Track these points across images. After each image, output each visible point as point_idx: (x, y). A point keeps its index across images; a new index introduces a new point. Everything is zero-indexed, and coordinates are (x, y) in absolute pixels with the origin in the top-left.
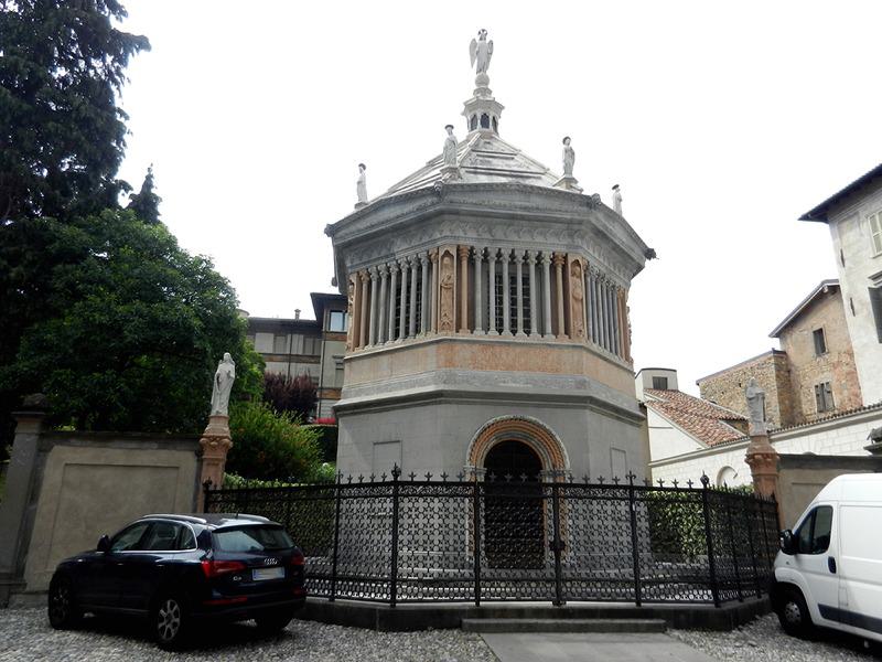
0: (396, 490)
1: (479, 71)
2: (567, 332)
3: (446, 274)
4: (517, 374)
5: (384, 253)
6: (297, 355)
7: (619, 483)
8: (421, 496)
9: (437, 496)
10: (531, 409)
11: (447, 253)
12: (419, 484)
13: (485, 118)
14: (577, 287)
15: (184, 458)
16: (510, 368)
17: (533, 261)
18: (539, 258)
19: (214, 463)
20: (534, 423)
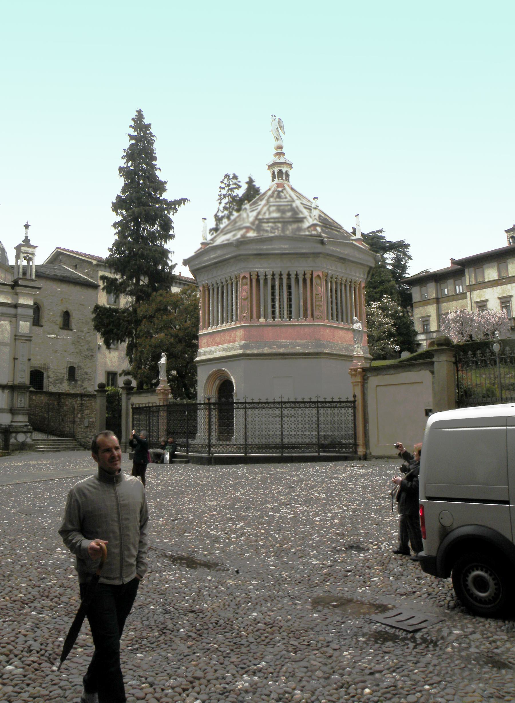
11: (244, 277)
13: (280, 172)
17: (293, 277)
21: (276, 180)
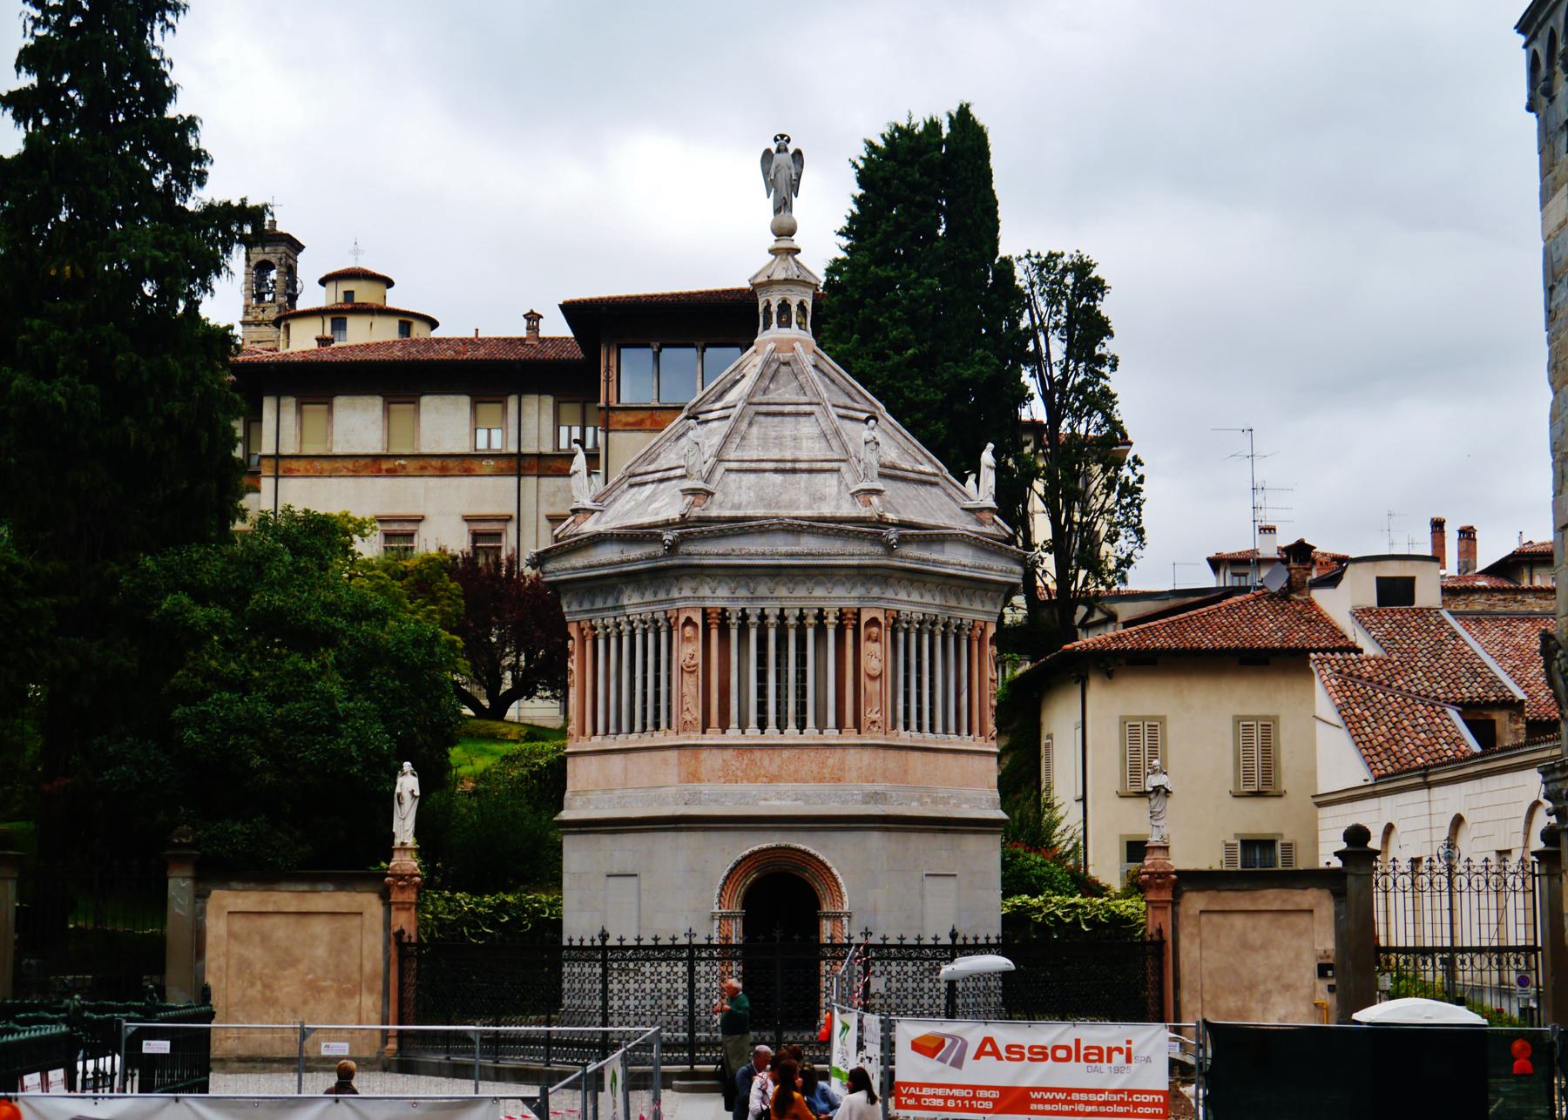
0: (604, 955)
1: (777, 211)
2: (857, 724)
3: (688, 651)
4: (783, 787)
5: (610, 603)
6: (540, 456)
8: (631, 960)
11: (689, 621)
12: (628, 948)
14: (874, 656)
15: (369, 903)
16: (773, 779)
18: (821, 616)
19: (404, 906)
20: (804, 852)
21: (774, 325)
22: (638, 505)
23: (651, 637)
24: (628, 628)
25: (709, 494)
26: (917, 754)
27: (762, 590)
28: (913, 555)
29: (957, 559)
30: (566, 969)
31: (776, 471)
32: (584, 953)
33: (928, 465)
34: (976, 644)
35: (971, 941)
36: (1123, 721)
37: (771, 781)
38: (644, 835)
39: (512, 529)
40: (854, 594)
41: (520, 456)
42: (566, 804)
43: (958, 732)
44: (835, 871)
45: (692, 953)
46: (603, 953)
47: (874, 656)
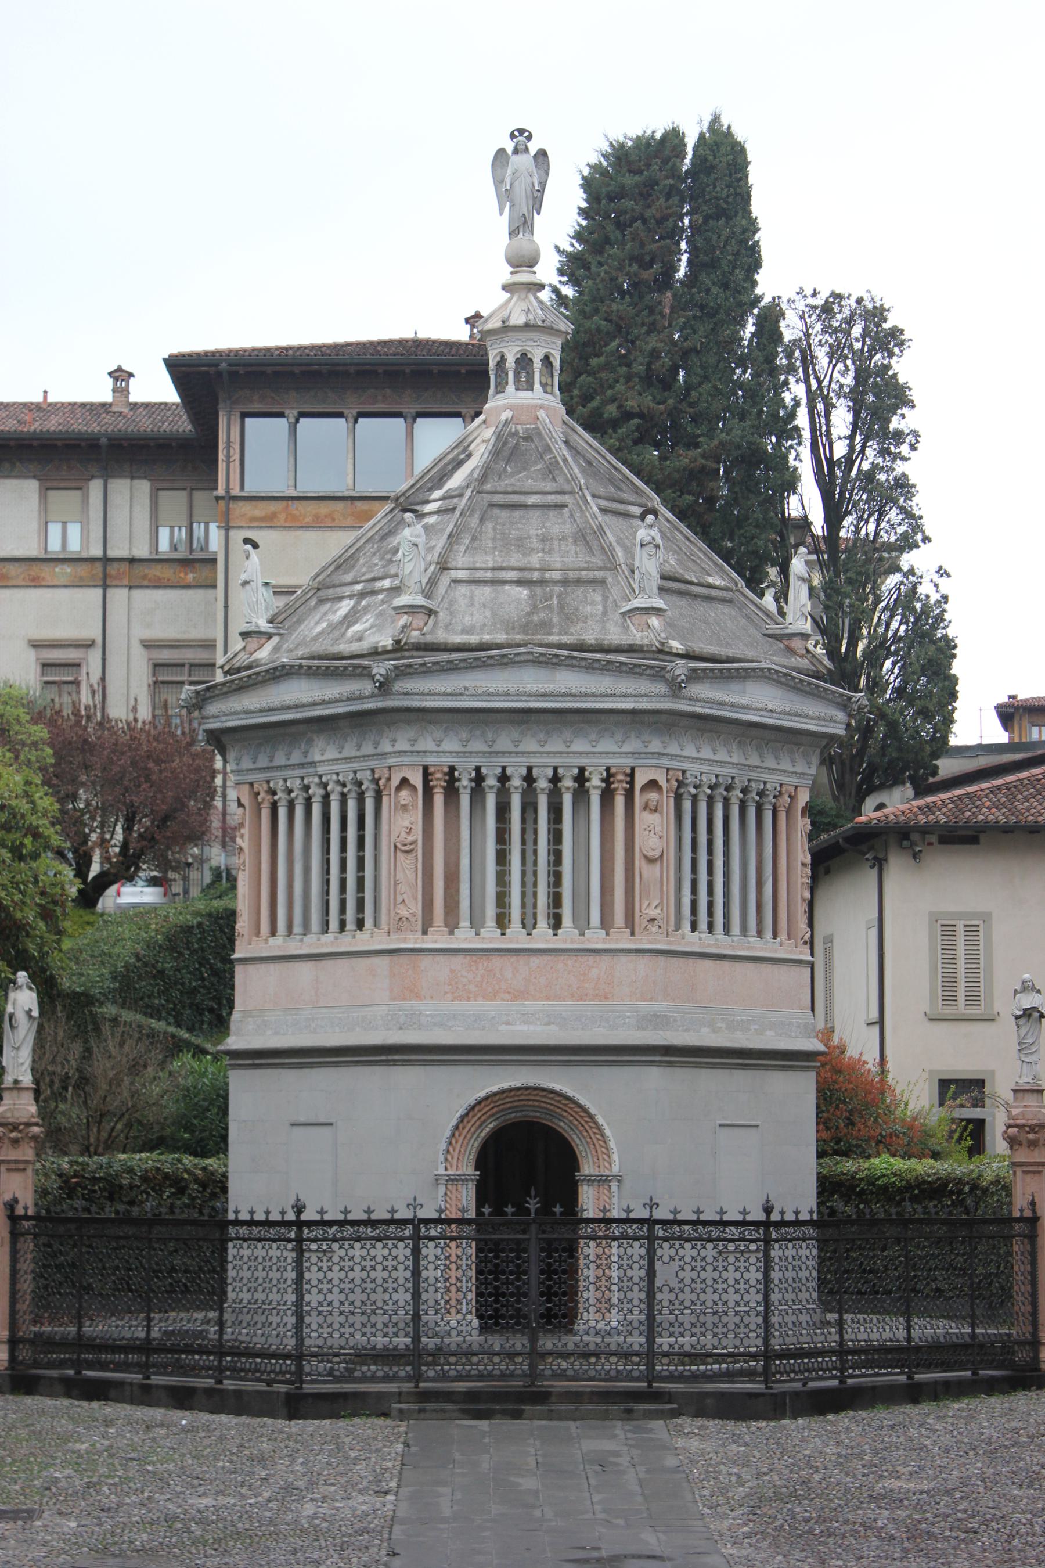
1: (513, 233)
4: (531, 1006)
5: (296, 757)
7: (632, 1216)
8: (335, 1240)
9: (358, 1239)
10: (555, 1070)
11: (404, 781)
12: (330, 1223)
16: (519, 995)
18: (581, 778)
21: (511, 388)
22: (333, 627)
23: (352, 805)
24: (322, 792)
25: (431, 612)
26: (708, 963)
27: (504, 743)
28: (707, 696)
29: (761, 702)
30: (232, 1251)
31: (519, 582)
32: (264, 1228)
33: (719, 576)
34: (782, 816)
35: (790, 1217)
36: (934, 918)
37: (515, 998)
38: (343, 1070)
39: (94, 658)
40: (627, 748)
41: (106, 560)
42: (233, 1027)
43: (760, 933)
44: (600, 1120)
45: (416, 1229)
46: (298, 1231)
47: (654, 830)
